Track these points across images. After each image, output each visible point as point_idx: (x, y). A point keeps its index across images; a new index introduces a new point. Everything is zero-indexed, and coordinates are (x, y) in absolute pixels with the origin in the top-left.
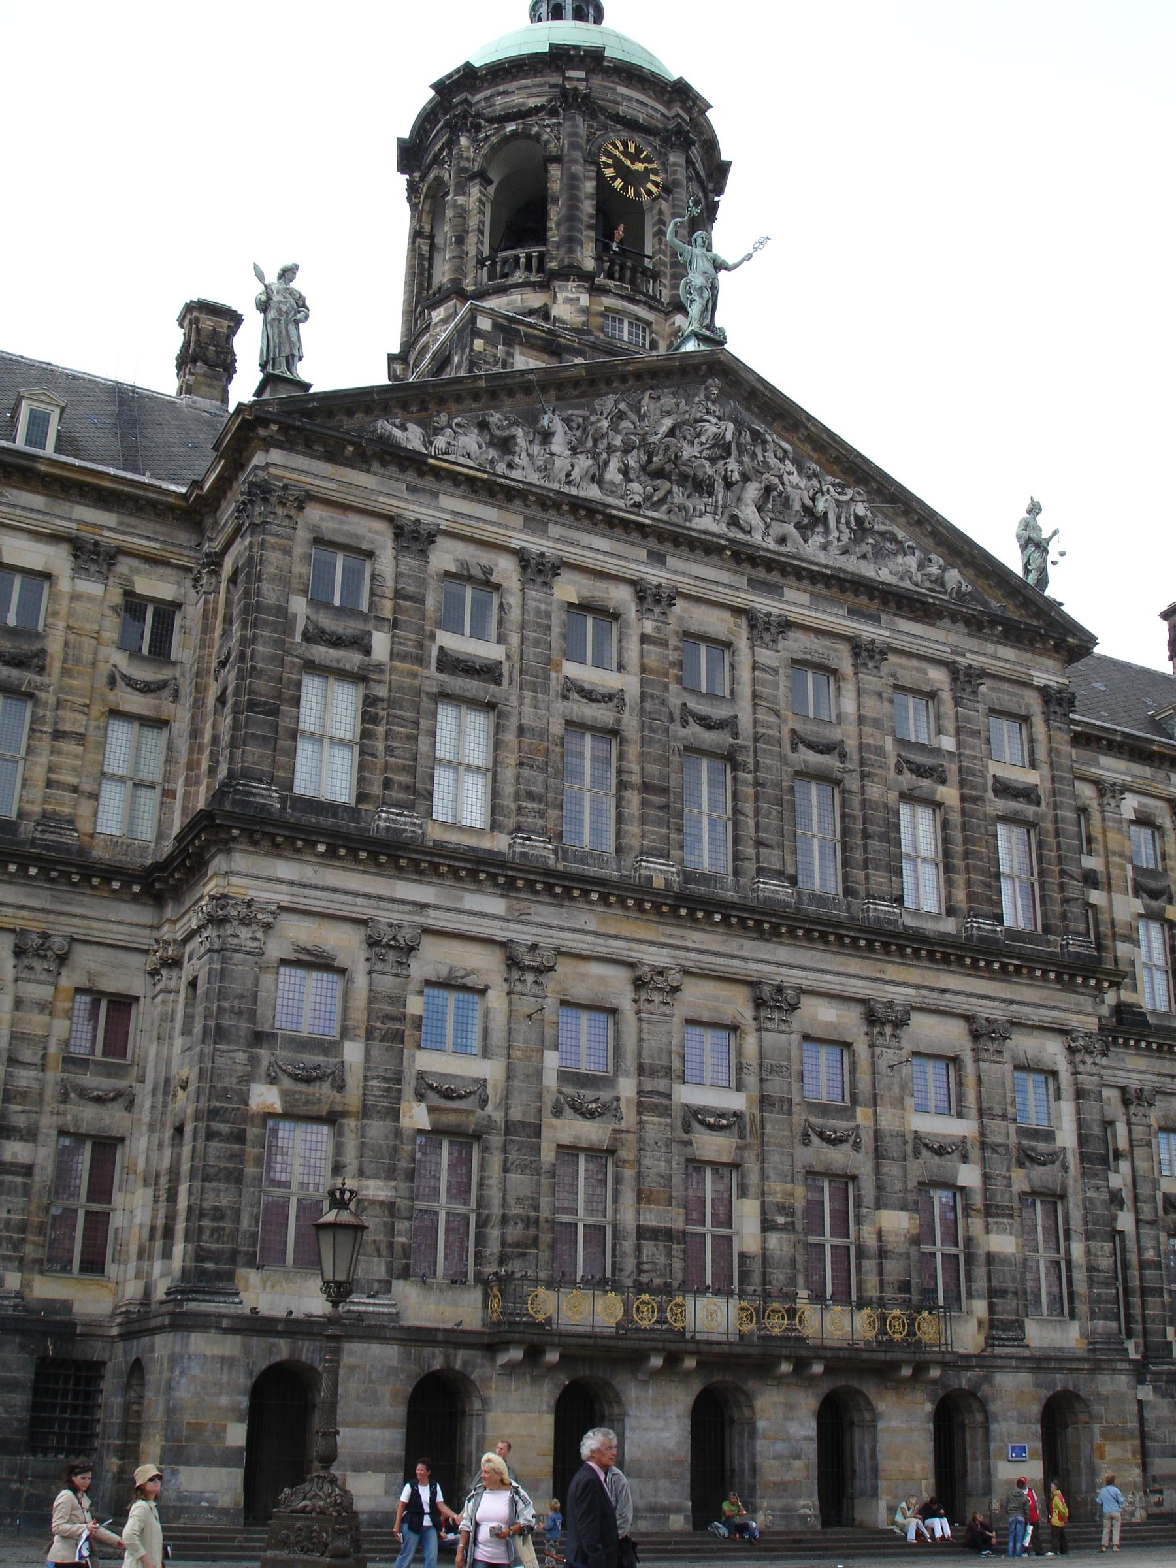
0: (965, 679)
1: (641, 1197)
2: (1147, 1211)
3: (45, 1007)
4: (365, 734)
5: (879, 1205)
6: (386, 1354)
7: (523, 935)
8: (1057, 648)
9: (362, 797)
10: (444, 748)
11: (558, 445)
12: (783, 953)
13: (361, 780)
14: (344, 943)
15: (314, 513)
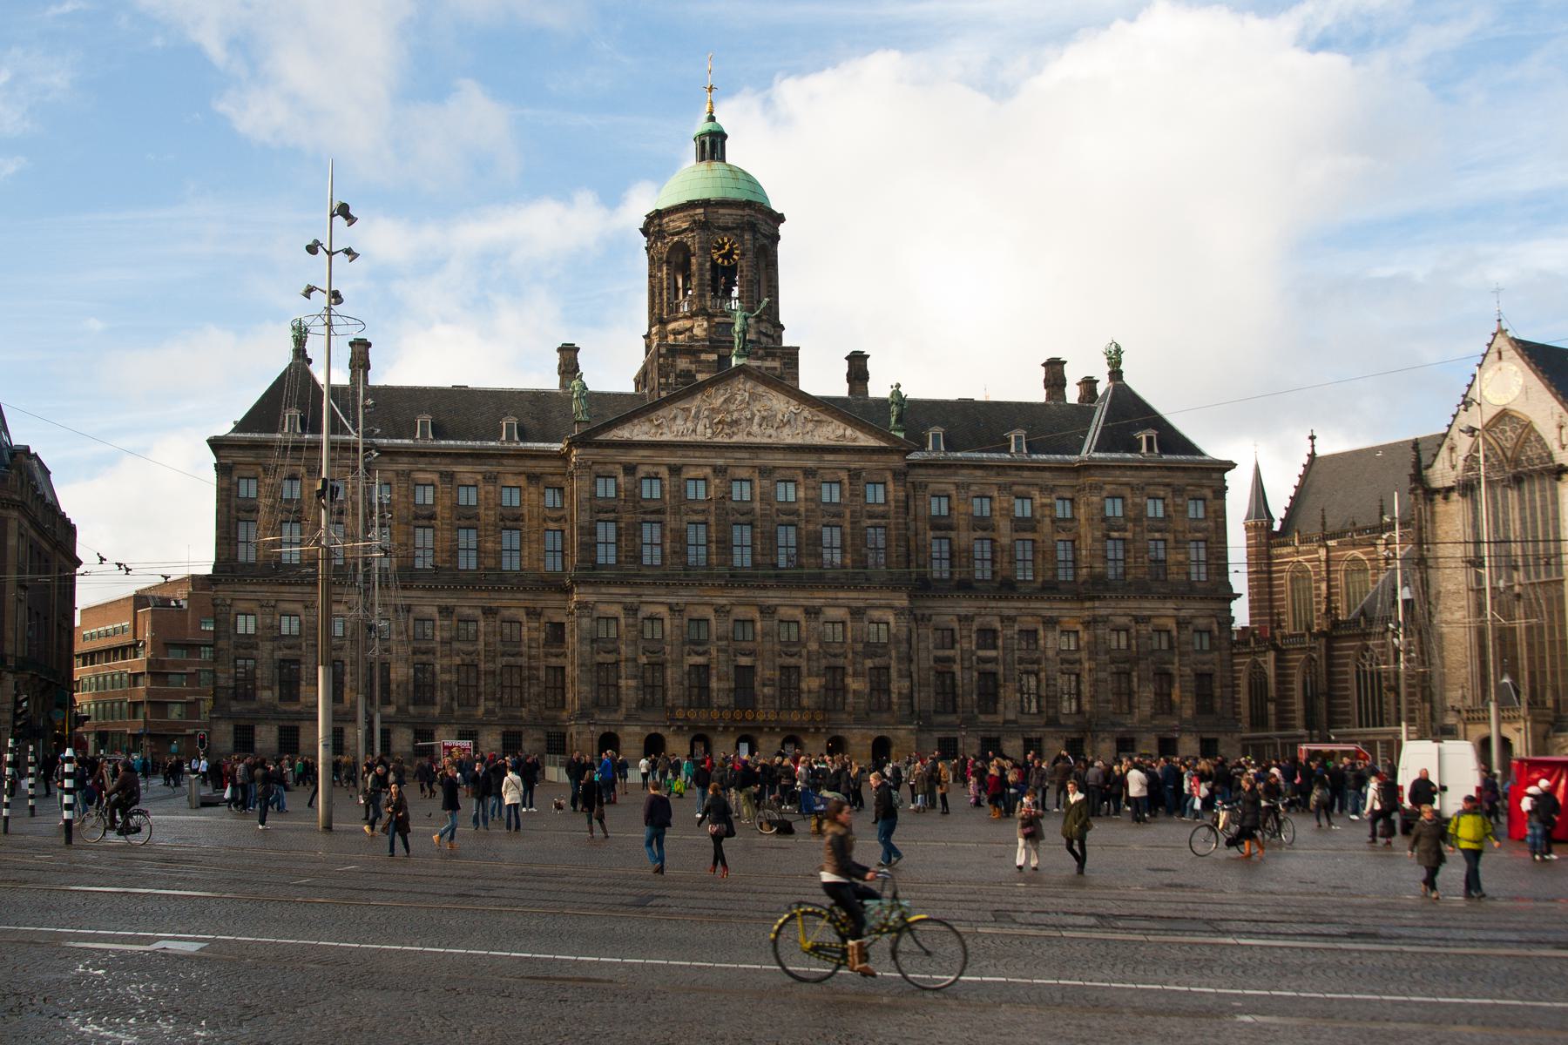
0: (855, 475)
1: (719, 679)
2: (967, 664)
3: (537, 629)
4: (618, 540)
5: (809, 675)
6: (638, 729)
7: (672, 600)
8: (898, 451)
9: (618, 562)
10: (646, 539)
11: (679, 421)
12: (771, 594)
13: (617, 556)
14: (615, 610)
15: (596, 467)
